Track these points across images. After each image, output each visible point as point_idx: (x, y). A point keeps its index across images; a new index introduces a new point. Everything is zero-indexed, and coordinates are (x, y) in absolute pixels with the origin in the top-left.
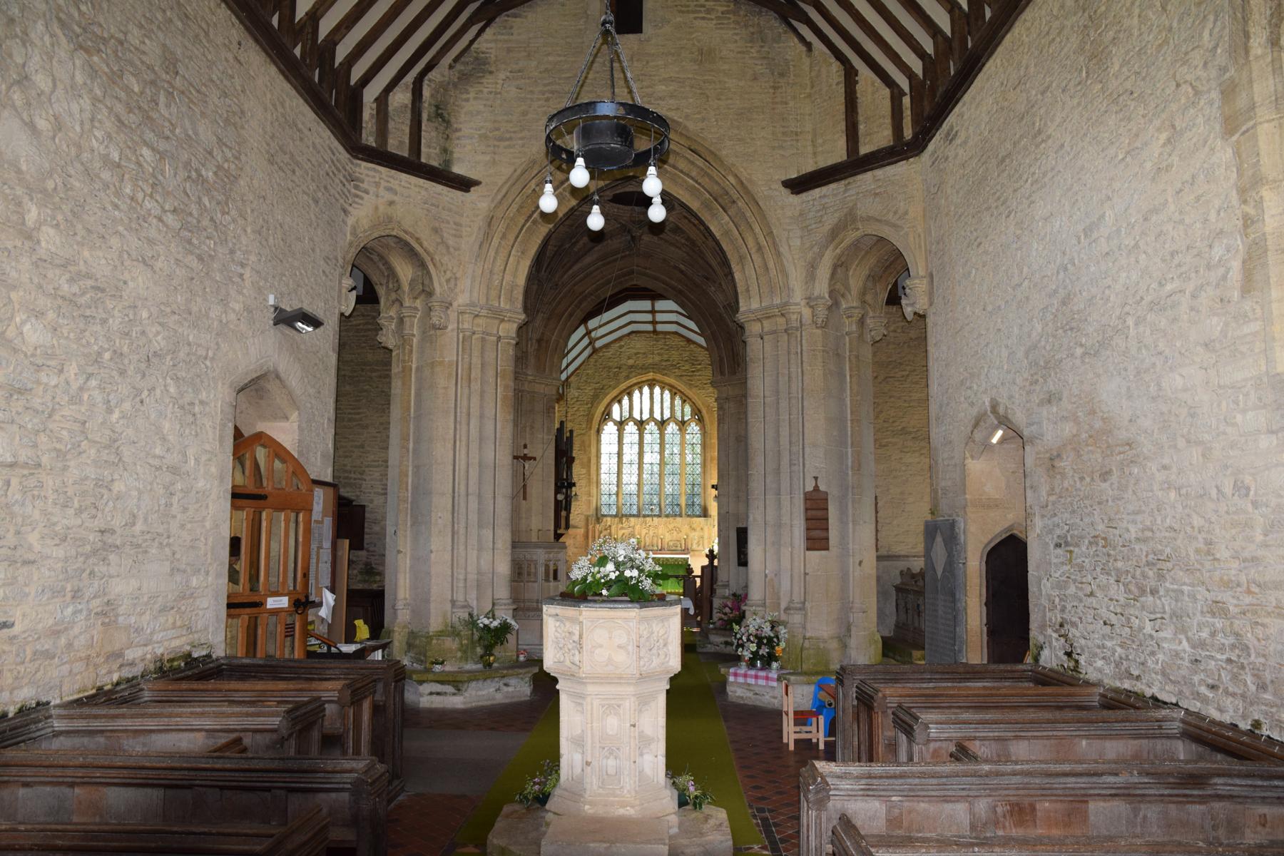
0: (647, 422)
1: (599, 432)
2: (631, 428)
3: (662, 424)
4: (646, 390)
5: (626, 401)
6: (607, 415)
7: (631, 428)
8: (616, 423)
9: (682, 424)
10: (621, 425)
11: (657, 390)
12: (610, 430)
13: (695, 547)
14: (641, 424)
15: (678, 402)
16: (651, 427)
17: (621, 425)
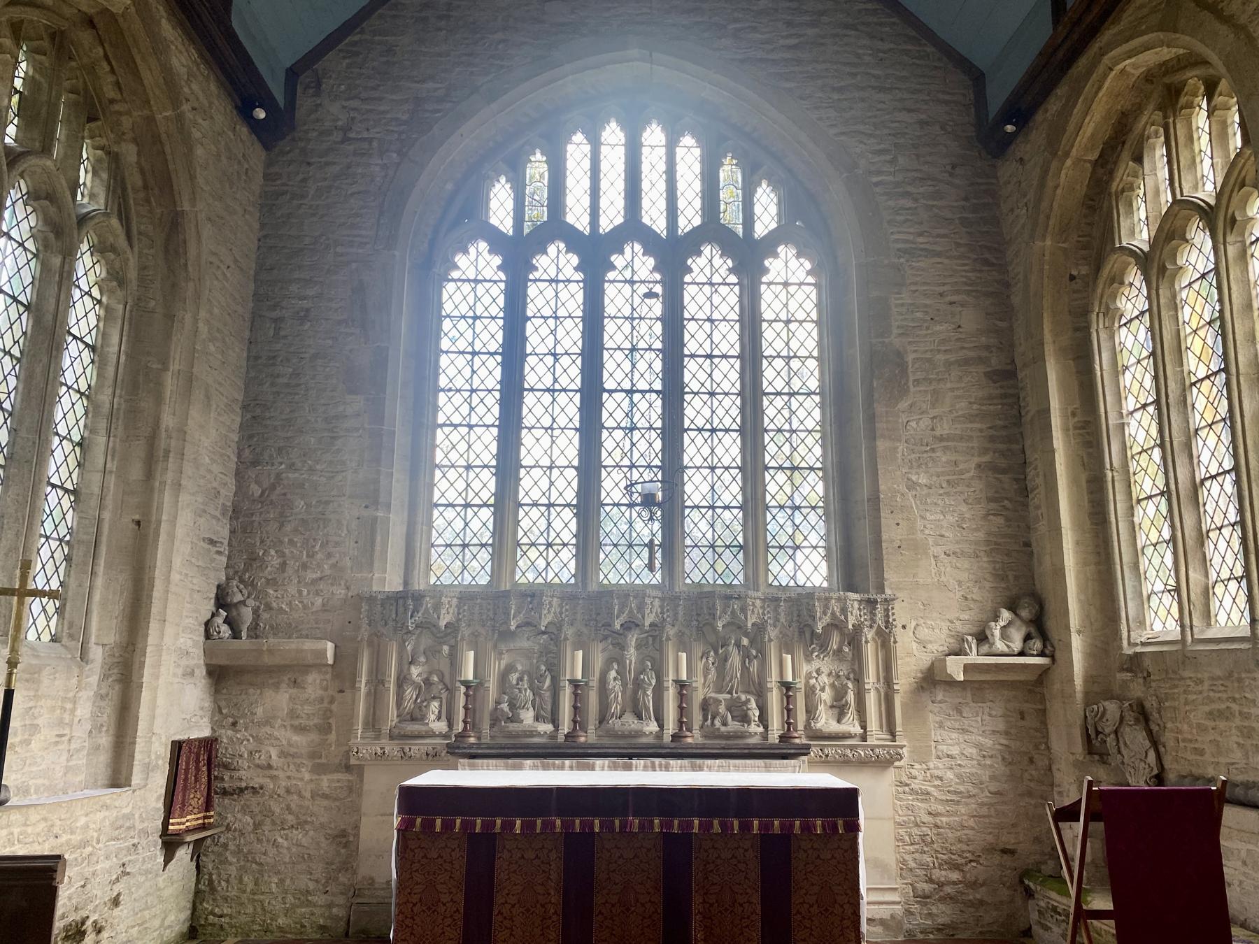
0: (617, 240)
1: (432, 271)
2: (558, 261)
3: (673, 254)
4: (613, 134)
5: (537, 168)
6: (467, 219)
7: (558, 261)
8: (497, 241)
9: (748, 258)
10: (517, 256)
11: (654, 136)
12: (478, 263)
13: (826, 721)
14: (595, 254)
15: (729, 172)
16: (635, 263)
17: (517, 256)
